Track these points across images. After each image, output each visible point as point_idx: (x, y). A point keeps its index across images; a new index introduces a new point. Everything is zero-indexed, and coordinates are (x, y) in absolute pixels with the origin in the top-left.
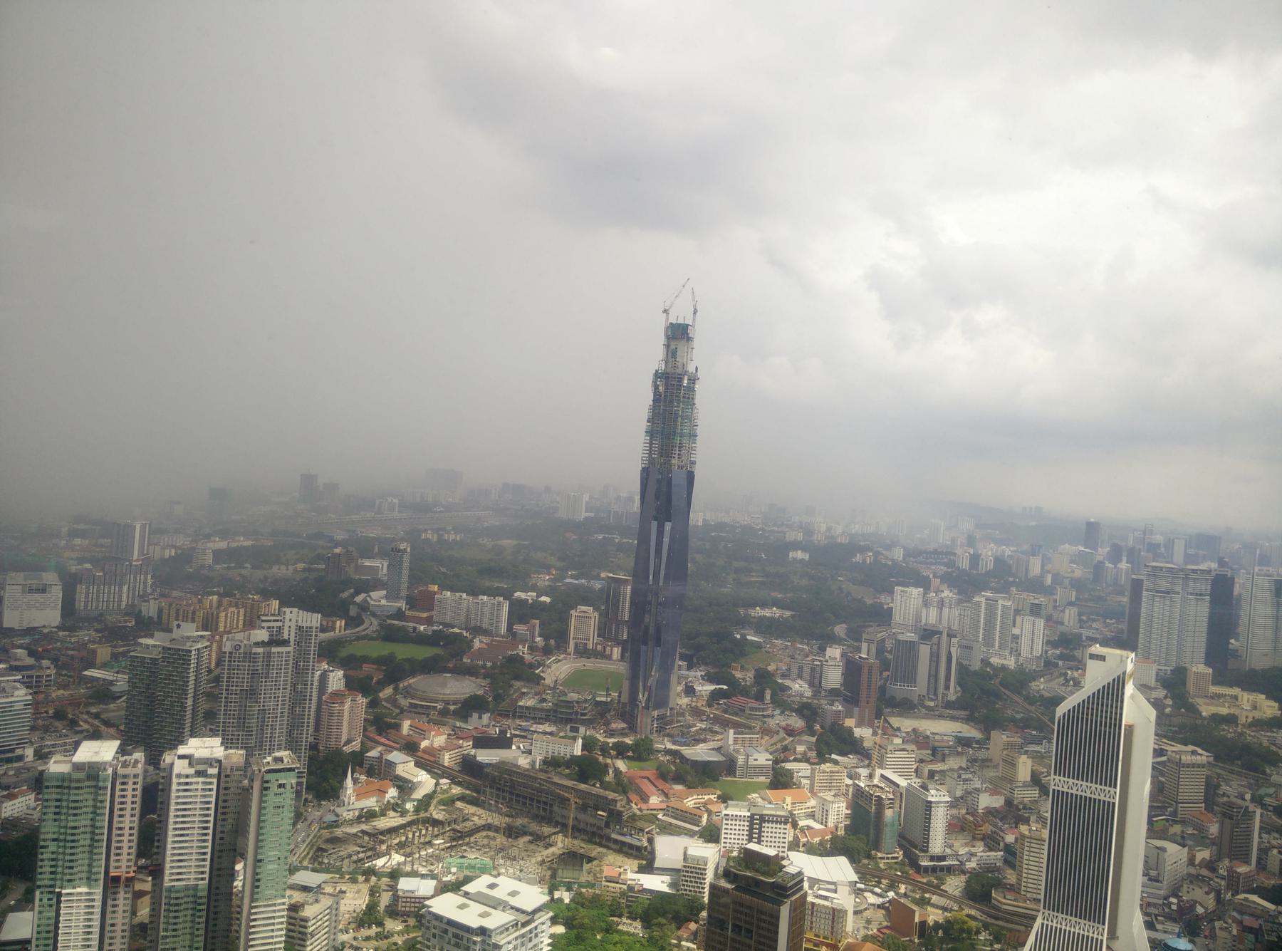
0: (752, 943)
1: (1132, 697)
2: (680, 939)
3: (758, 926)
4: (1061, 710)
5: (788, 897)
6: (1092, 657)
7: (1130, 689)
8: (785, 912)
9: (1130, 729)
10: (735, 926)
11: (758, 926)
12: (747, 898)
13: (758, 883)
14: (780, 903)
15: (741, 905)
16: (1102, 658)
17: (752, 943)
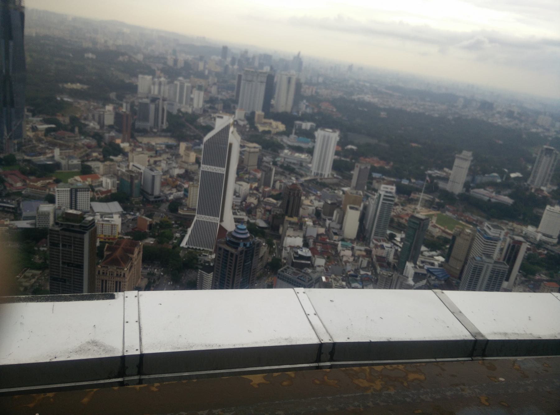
0: (72, 250)
1: (232, 132)
2: (39, 248)
3: (74, 244)
4: (206, 139)
5: (87, 230)
6: (218, 117)
7: (232, 129)
8: (86, 237)
9: (231, 145)
10: (64, 246)
11: (74, 244)
12: (67, 233)
13: (73, 226)
14: (84, 233)
15: (65, 236)
16: (222, 117)
17: (72, 250)
